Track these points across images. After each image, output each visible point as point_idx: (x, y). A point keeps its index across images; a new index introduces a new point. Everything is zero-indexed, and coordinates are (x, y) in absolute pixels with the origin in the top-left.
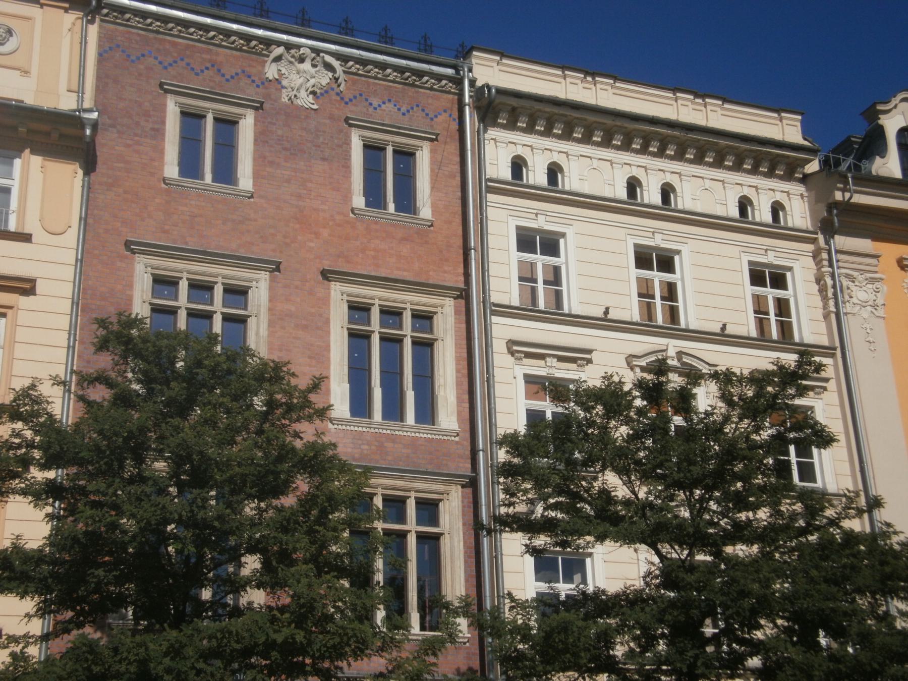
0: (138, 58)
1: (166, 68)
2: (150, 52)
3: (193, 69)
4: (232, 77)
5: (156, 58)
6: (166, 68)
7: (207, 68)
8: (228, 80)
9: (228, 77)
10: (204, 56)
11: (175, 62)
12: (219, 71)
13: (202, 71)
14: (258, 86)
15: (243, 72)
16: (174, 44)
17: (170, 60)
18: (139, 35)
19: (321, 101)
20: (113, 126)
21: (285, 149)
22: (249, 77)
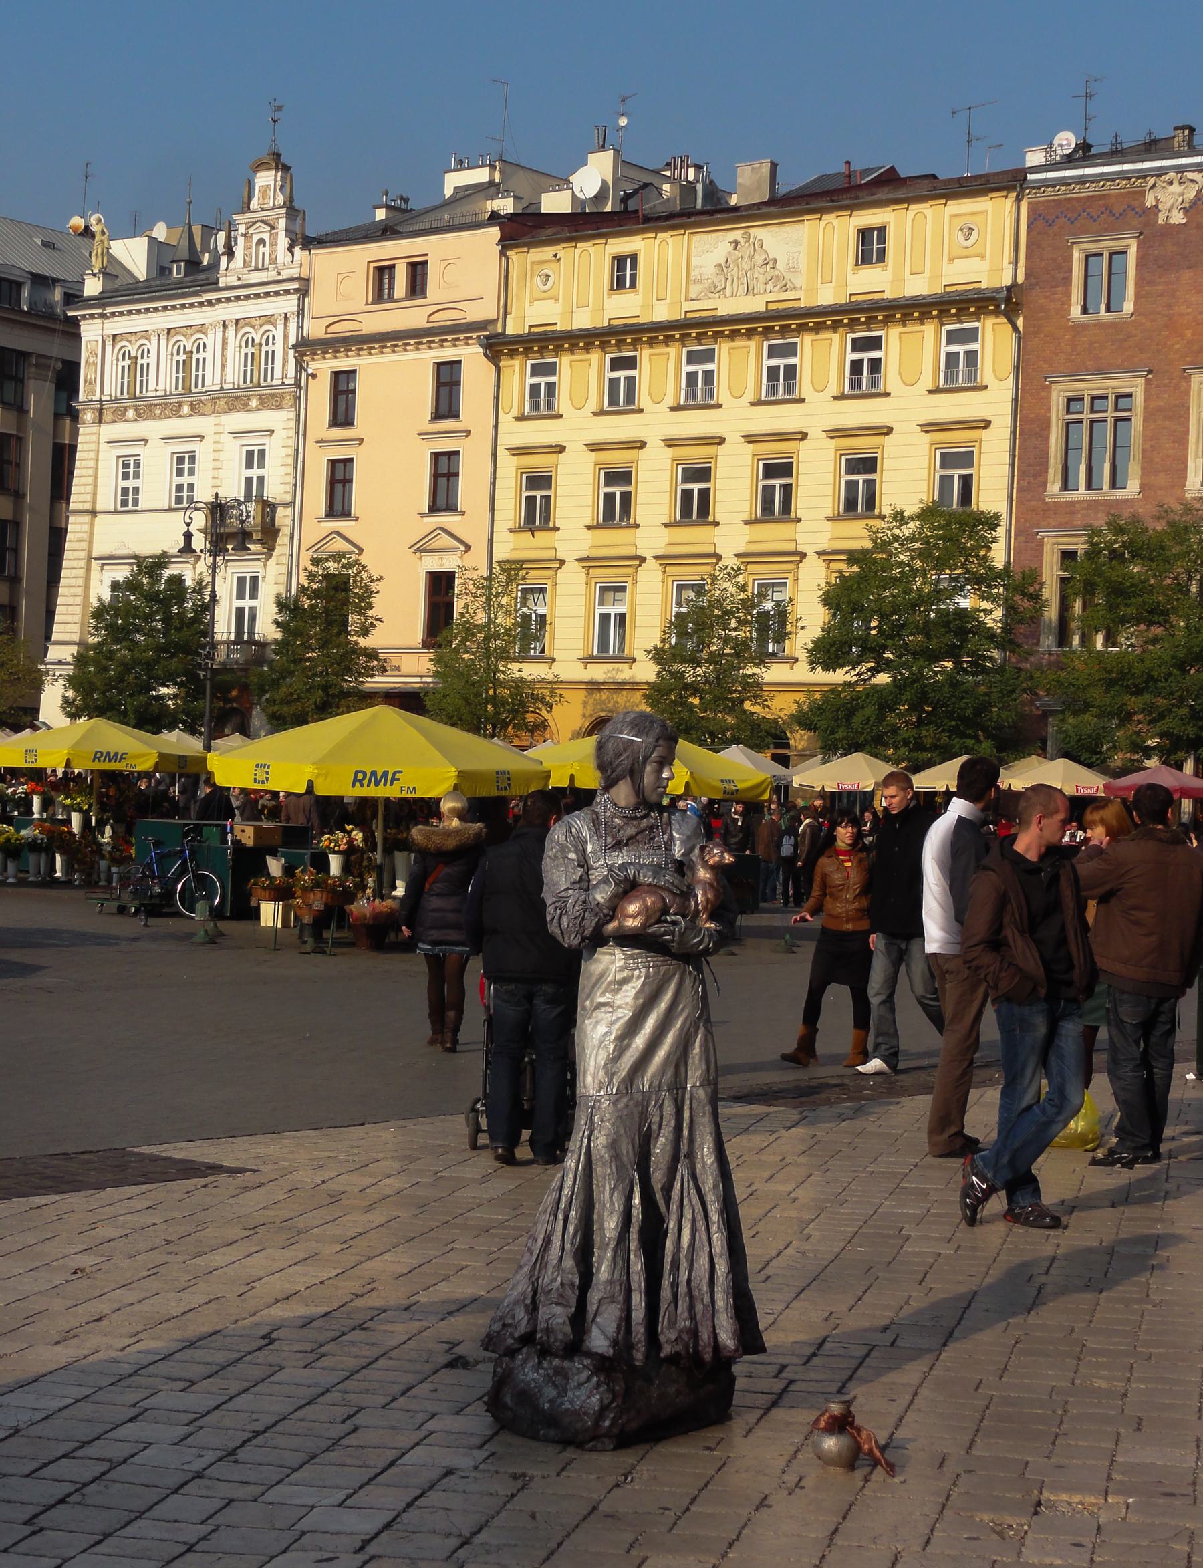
0: (1053, 221)
1: (1072, 223)
2: (1062, 213)
3: (1091, 217)
4: (1121, 214)
5: (1066, 217)
6: (1072, 223)
7: (1102, 213)
8: (1117, 218)
9: (1117, 215)
10: (1100, 202)
11: (1079, 215)
12: (1111, 212)
13: (1099, 216)
14: (1140, 216)
15: (1129, 206)
16: (1078, 199)
17: (1076, 215)
18: (1054, 200)
19: (1189, 214)
20: (1037, 284)
21: (1160, 267)
22: (1133, 209)
